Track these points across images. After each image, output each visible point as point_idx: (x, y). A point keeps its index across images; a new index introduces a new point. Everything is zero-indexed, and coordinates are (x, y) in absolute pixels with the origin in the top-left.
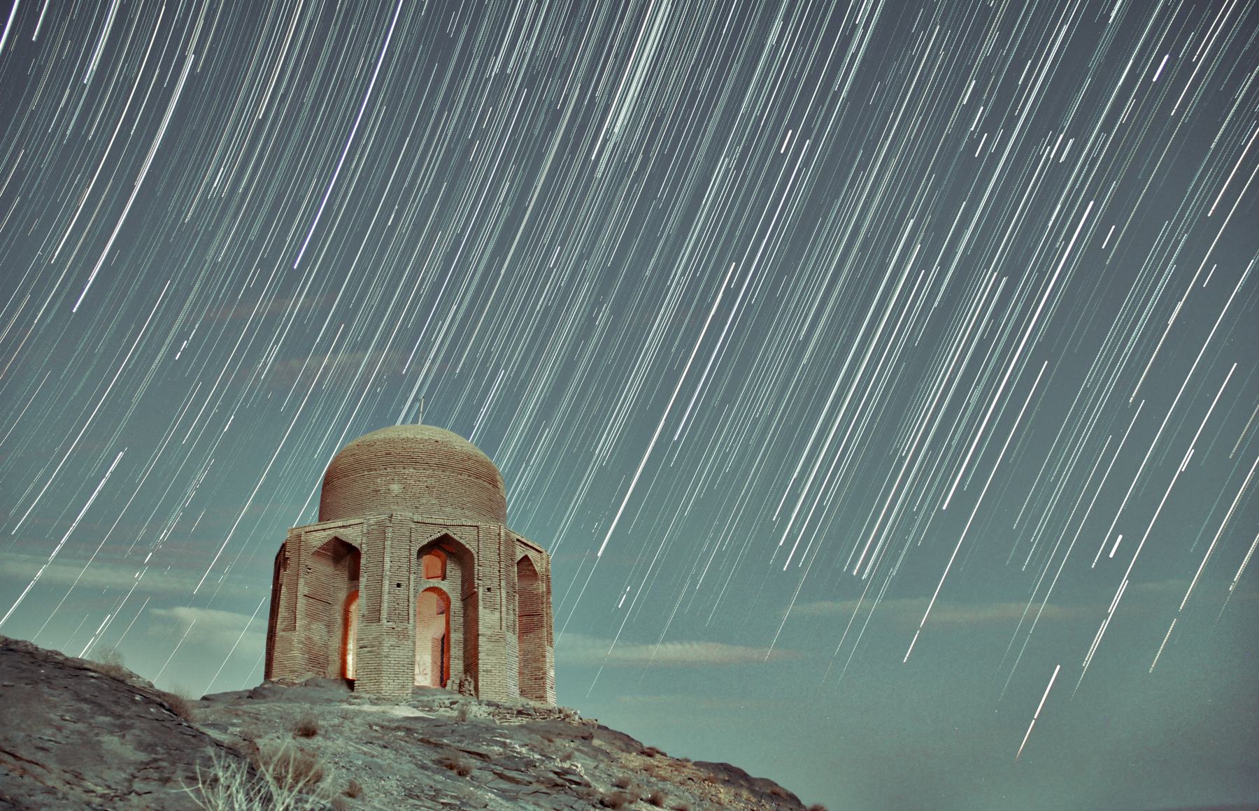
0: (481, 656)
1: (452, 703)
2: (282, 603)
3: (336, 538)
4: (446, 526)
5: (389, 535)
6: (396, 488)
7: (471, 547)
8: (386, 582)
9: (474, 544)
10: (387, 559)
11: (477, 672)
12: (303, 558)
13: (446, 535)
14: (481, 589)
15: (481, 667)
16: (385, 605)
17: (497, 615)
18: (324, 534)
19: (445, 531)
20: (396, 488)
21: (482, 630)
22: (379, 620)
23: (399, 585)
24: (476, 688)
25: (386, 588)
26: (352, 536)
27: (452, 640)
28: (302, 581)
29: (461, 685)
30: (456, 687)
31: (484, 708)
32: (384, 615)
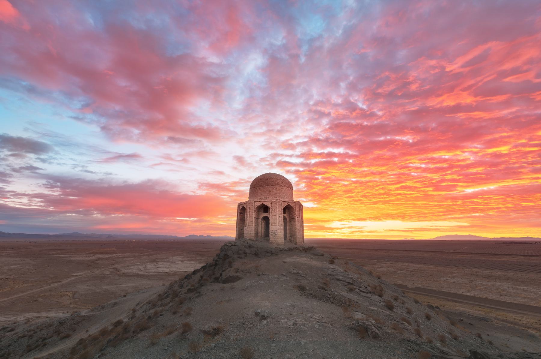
3: (263, 204)
13: (289, 205)
26: (268, 204)
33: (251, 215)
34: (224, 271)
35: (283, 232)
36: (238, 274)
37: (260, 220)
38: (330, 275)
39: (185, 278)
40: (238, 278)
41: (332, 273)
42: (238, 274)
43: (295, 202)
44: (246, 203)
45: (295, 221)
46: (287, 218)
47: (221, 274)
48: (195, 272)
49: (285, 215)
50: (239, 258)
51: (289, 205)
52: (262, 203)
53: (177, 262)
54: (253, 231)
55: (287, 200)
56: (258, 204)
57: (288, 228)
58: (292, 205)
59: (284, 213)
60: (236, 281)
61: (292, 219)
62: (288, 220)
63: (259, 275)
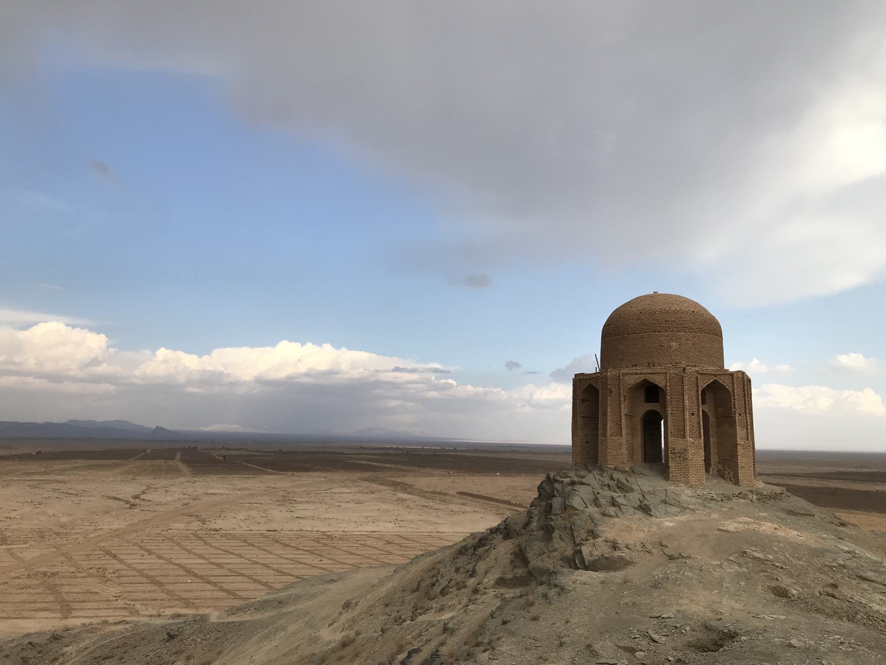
2: (609, 418)
3: (645, 381)
7: (729, 387)
8: (687, 413)
10: (686, 398)
11: (738, 467)
14: (737, 415)
18: (637, 377)
21: (739, 441)
22: (684, 436)
23: (693, 414)
25: (687, 417)
26: (659, 380)
29: (719, 471)
31: (755, 497)
38: (844, 566)
40: (624, 563)
42: (617, 553)
43: (732, 374)
45: (733, 424)
46: (710, 415)
50: (604, 514)
52: (643, 377)
53: (344, 505)
54: (624, 447)
55: (711, 368)
56: (633, 380)
58: (726, 382)
62: (712, 420)
63: (671, 558)
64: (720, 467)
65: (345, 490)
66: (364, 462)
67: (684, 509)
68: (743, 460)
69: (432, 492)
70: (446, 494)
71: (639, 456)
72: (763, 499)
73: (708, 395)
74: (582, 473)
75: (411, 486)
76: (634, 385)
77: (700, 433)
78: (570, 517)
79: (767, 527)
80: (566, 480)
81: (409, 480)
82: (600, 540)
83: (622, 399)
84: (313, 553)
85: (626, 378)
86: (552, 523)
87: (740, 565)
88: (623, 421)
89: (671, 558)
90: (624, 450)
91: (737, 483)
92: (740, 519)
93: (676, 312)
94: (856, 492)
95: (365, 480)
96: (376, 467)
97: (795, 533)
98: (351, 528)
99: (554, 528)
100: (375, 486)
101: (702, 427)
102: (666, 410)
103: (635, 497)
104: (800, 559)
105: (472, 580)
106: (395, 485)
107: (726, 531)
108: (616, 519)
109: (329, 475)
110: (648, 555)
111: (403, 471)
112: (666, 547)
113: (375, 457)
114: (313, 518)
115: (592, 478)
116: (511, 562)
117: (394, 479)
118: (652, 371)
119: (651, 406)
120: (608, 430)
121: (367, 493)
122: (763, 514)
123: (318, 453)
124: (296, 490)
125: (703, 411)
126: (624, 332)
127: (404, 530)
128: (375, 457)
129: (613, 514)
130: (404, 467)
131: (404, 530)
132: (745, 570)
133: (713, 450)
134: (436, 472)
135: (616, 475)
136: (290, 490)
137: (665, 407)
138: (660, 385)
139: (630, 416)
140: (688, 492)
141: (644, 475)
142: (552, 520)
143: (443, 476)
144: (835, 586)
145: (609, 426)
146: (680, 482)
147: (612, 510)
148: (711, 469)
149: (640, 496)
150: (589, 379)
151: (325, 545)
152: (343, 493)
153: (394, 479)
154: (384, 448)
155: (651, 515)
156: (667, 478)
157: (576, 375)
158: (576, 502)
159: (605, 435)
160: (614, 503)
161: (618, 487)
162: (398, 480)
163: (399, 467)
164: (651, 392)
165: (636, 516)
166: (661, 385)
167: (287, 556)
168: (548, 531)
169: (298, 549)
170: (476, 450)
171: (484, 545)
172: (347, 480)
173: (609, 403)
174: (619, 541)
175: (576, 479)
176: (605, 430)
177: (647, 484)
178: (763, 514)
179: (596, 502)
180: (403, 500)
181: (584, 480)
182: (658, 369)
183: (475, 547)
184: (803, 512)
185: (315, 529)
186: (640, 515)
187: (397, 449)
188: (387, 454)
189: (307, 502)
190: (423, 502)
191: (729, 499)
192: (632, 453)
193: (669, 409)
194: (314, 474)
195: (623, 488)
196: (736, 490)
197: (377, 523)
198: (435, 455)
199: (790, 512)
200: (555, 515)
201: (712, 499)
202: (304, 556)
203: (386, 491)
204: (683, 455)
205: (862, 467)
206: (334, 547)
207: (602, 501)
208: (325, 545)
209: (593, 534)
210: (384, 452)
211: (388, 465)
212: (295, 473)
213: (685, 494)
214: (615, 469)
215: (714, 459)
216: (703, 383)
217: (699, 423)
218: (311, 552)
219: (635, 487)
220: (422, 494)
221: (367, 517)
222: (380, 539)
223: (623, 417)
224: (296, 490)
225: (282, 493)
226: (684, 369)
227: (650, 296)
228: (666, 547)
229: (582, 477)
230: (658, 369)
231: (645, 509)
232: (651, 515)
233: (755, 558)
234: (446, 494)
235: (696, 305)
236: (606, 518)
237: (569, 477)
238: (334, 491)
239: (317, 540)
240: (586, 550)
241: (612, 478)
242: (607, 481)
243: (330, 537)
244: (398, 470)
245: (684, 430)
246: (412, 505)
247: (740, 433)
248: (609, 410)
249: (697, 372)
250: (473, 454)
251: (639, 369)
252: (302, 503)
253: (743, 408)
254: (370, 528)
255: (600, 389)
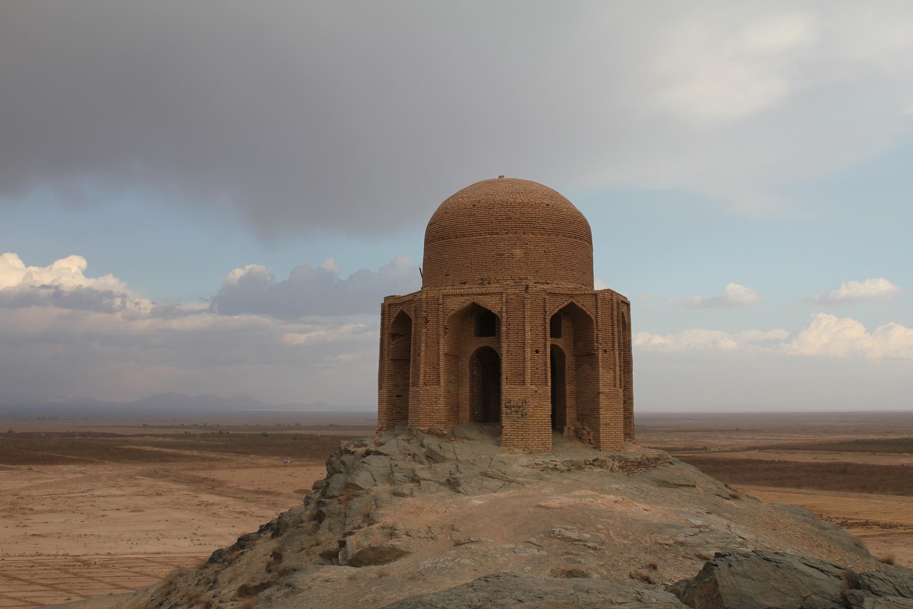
0: (602, 411)
1: (594, 460)
2: (423, 359)
3: (474, 305)
4: (571, 296)
5: (528, 306)
6: (518, 252)
7: (591, 312)
8: (528, 350)
9: (593, 310)
10: (528, 329)
11: (598, 425)
12: (441, 319)
13: (572, 305)
14: (600, 352)
15: (602, 421)
16: (528, 371)
17: (612, 372)
18: (462, 299)
19: (570, 301)
20: (518, 252)
21: (602, 389)
23: (537, 351)
24: (597, 439)
25: (528, 355)
26: (492, 304)
27: (568, 392)
28: (442, 341)
29: (576, 431)
30: (572, 434)
31: (616, 464)
32: (528, 381)
33: (434, 348)
34: (351, 534)
35: (548, 405)
36: (394, 542)
37: (465, 364)
38: (682, 544)
39: (212, 560)
40: (397, 554)
41: (689, 539)
42: (394, 542)
43: (596, 295)
44: (412, 299)
45: (594, 366)
46: (568, 353)
47: (343, 544)
48: (244, 542)
49: (560, 342)
50: (396, 494)
51: (572, 305)
54: (442, 400)
55: (566, 286)
56: (456, 305)
57: (569, 388)
58: (586, 305)
59: (555, 333)
60: (389, 561)
61: (587, 357)
62: (569, 360)
63: (458, 544)
64: (579, 425)
65: (114, 491)
66: (148, 448)
67: (508, 481)
68: (608, 414)
69: (256, 492)
70: (279, 494)
71: (465, 414)
72: (630, 467)
73: (566, 327)
74: (382, 440)
75: (221, 483)
76: (460, 311)
77: (546, 377)
78: (348, 499)
79: (605, 501)
80: (361, 450)
81: (220, 474)
82: (374, 527)
83: (441, 332)
84: (57, 589)
85: (448, 301)
86: (324, 509)
87: (540, 547)
88: (442, 364)
89: (458, 544)
90: (442, 405)
91: (597, 448)
92: (577, 493)
93: (523, 205)
94: (887, 470)
95: (149, 475)
96: (168, 455)
97: (641, 506)
98: (121, 549)
99: (324, 516)
100: (163, 484)
101: (549, 370)
102: (500, 347)
103: (443, 469)
104: (626, 537)
105: (212, 592)
106: (196, 482)
107: (546, 507)
108: (409, 499)
109: (90, 469)
110: (431, 542)
111: (211, 460)
112: (457, 530)
113: (168, 439)
114: (59, 535)
115: (393, 444)
116: (269, 565)
117: (194, 473)
118: (483, 290)
119: (485, 342)
120: (422, 377)
121: (150, 496)
122: (617, 486)
123: (73, 435)
124: (34, 493)
125: (553, 346)
126: (455, 234)
127: (202, 548)
128: (168, 439)
129: (407, 492)
130: (212, 455)
131: (202, 548)
132: (544, 553)
133: (570, 402)
134: (264, 461)
135: (429, 441)
136: (23, 493)
137: (499, 342)
138: (494, 311)
139: (454, 357)
140: (524, 460)
141: (468, 439)
142: (324, 504)
143: (275, 466)
144: (654, 567)
145: (422, 371)
146: (516, 446)
147: (406, 488)
148: (566, 429)
149: (452, 468)
150: (401, 304)
151: (77, 575)
152: (114, 496)
153: (194, 473)
154: (183, 427)
155: (459, 492)
156: (499, 444)
157: (386, 298)
158: (362, 479)
159: (416, 384)
160: (415, 480)
161: (428, 457)
162: (202, 474)
163: (206, 454)
164: (485, 321)
165: (440, 493)
166: (495, 311)
167: (11, 595)
168: (319, 517)
169: (32, 583)
170: (332, 427)
171: (243, 547)
172: (118, 475)
173: (423, 338)
174: (400, 526)
175: (373, 448)
176: (417, 375)
177: (471, 450)
178: (617, 486)
179: (390, 478)
180: (208, 505)
181: (380, 449)
182: (494, 288)
183: (233, 548)
184: (682, 482)
185: (61, 552)
186: (445, 492)
187: (204, 427)
188: (187, 435)
189: (52, 511)
190: (240, 506)
191: (579, 467)
192: (454, 411)
193: (504, 345)
194: (65, 468)
195: (431, 457)
196: (591, 455)
197: (163, 540)
198: (265, 435)
199: (664, 483)
200: (331, 498)
201: (555, 469)
202: (42, 594)
203: (182, 492)
204: (520, 410)
205: (888, 432)
206: (90, 578)
207: (398, 476)
208: (77, 575)
209: (369, 519)
210: (182, 431)
211: (188, 452)
212: (34, 468)
213: (518, 462)
214: (430, 432)
215: (570, 414)
216: (553, 308)
217: (546, 364)
218: (53, 587)
219: (449, 455)
220: (240, 494)
221: (147, 532)
222: (166, 564)
223: (442, 357)
224: (34, 493)
225: (10, 498)
226: (527, 287)
227: (490, 182)
228: (457, 530)
229: (381, 444)
230: (494, 288)
231: (453, 484)
232: (459, 492)
233: (564, 539)
234: (279, 494)
235: (554, 195)
236: (396, 499)
237: (366, 445)
238: (96, 493)
239: (64, 569)
240: (350, 540)
241: (422, 446)
242: (413, 448)
243: (86, 564)
244: (204, 459)
245: (523, 374)
246: (221, 512)
247: (605, 377)
248: (423, 348)
249: (545, 290)
250: (324, 433)
251: (466, 289)
252: (41, 512)
253: (610, 342)
254: (152, 547)
255: (412, 317)
